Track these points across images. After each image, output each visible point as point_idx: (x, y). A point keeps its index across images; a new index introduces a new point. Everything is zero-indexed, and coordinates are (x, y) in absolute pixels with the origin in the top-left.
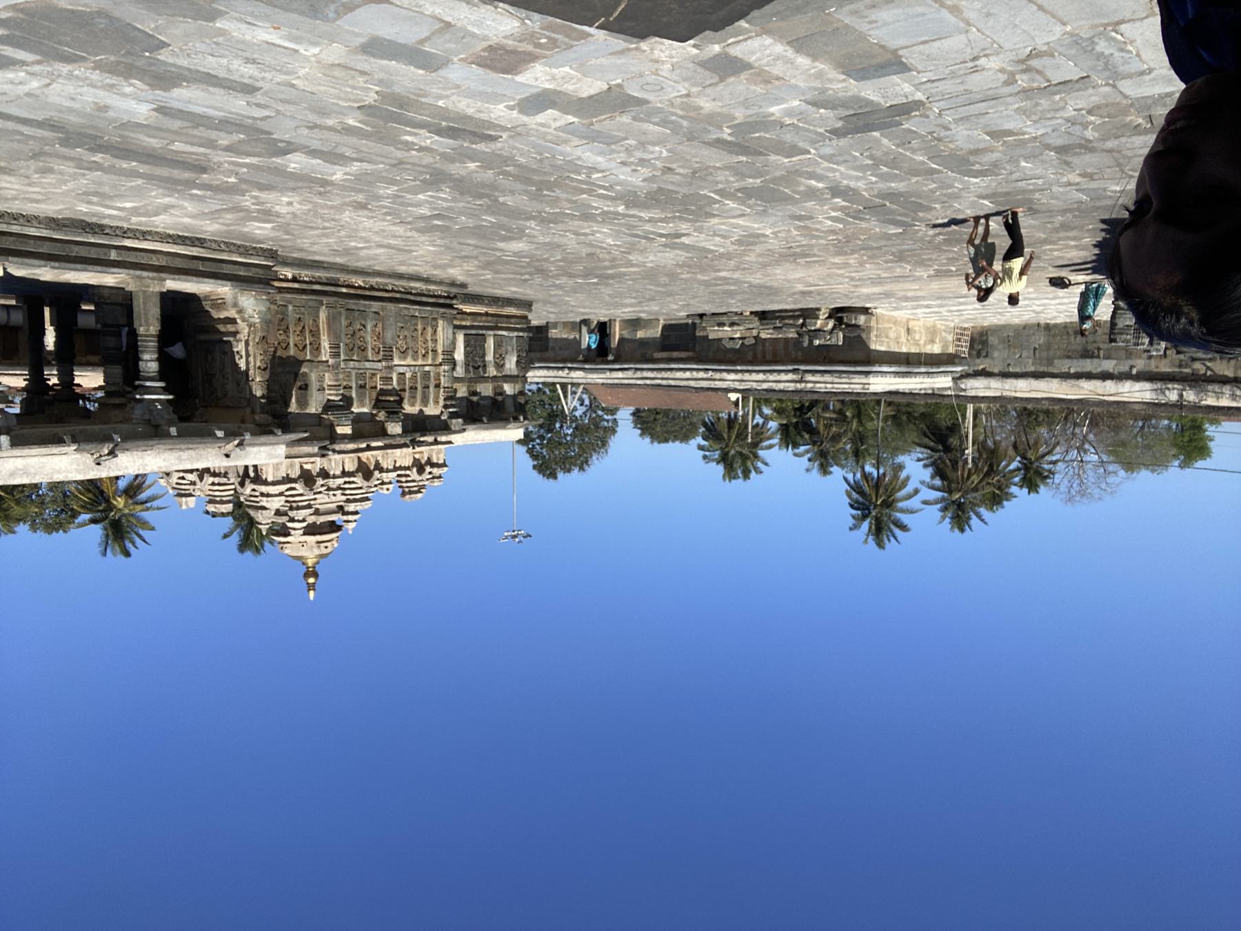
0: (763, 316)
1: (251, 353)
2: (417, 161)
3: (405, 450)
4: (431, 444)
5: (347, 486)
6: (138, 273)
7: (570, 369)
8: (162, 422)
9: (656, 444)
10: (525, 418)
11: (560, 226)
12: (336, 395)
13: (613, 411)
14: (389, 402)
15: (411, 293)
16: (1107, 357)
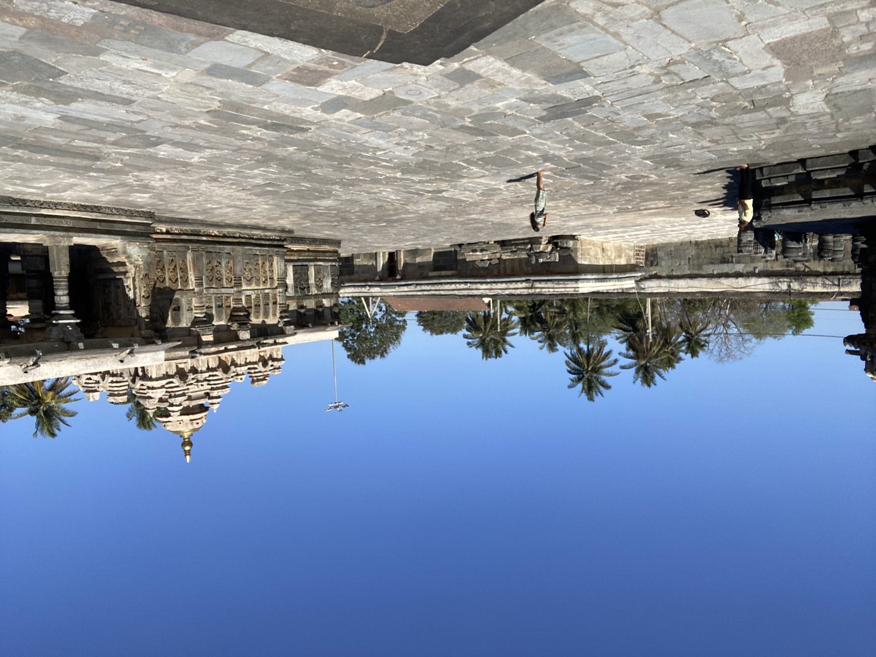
0: (503, 244)
1: (137, 286)
2: (252, 147)
3: (253, 350)
5: (211, 378)
6: (52, 233)
8: (72, 339)
9: (434, 335)
11: (357, 188)
12: (201, 313)
13: (402, 314)
14: (240, 316)
15: (253, 239)
16: (738, 262)
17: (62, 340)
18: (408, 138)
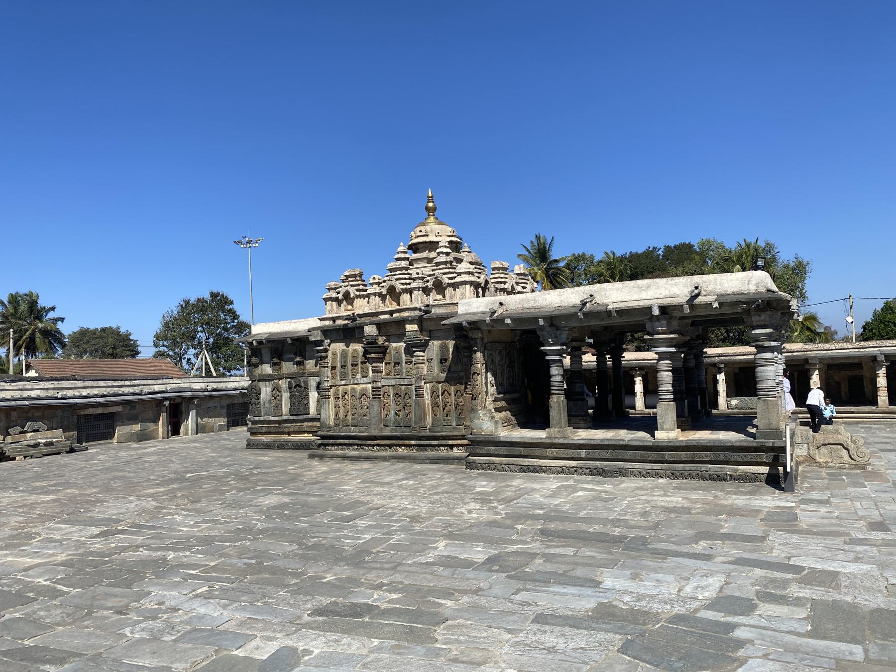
2: (381, 573)
3: (361, 312)
4: (339, 318)
5: (408, 281)
6: (566, 441)
7: (206, 390)
8: (548, 329)
10: (252, 343)
11: (232, 526)
12: (418, 356)
14: (375, 352)
15: (358, 445)
17: (558, 329)
18: (158, 624)
